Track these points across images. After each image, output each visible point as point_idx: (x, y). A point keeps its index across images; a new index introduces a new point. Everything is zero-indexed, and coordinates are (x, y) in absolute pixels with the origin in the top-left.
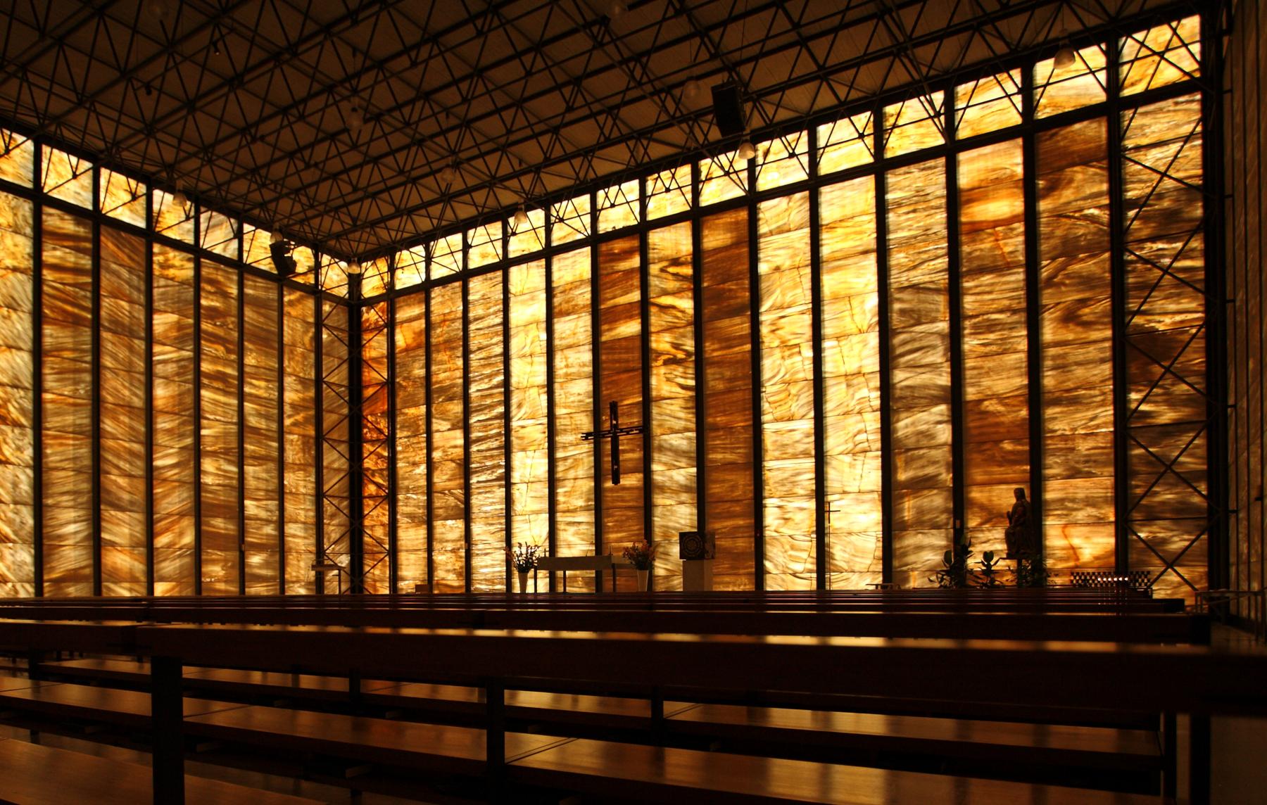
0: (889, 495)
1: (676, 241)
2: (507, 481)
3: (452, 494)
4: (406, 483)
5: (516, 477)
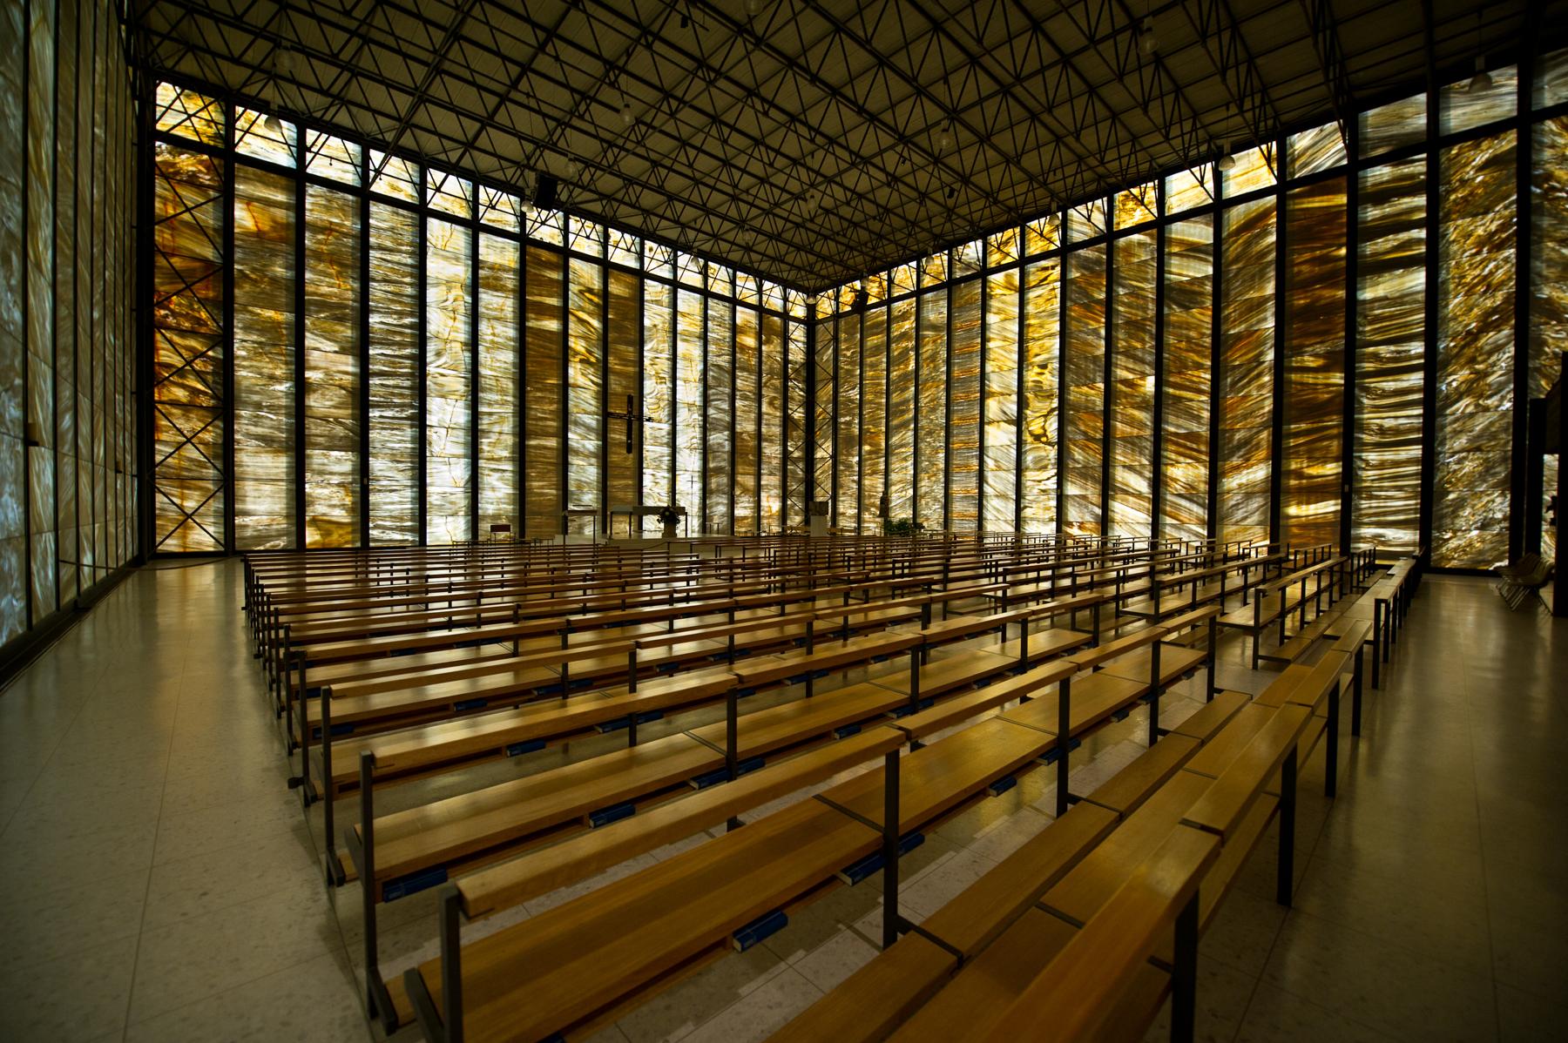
0: (705, 474)
1: (586, 274)
2: (420, 421)
3: (337, 421)
4: (256, 398)
5: (431, 420)
